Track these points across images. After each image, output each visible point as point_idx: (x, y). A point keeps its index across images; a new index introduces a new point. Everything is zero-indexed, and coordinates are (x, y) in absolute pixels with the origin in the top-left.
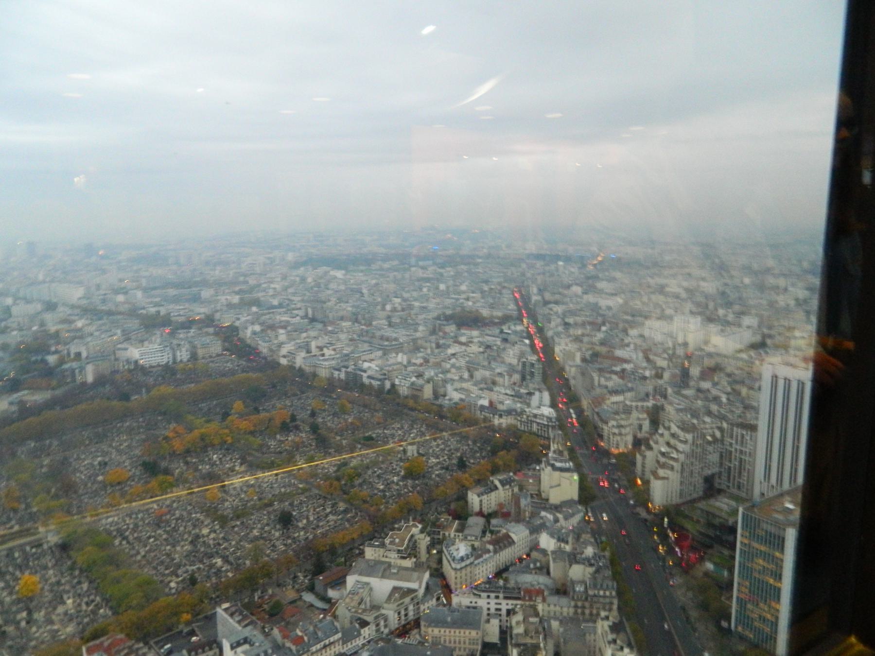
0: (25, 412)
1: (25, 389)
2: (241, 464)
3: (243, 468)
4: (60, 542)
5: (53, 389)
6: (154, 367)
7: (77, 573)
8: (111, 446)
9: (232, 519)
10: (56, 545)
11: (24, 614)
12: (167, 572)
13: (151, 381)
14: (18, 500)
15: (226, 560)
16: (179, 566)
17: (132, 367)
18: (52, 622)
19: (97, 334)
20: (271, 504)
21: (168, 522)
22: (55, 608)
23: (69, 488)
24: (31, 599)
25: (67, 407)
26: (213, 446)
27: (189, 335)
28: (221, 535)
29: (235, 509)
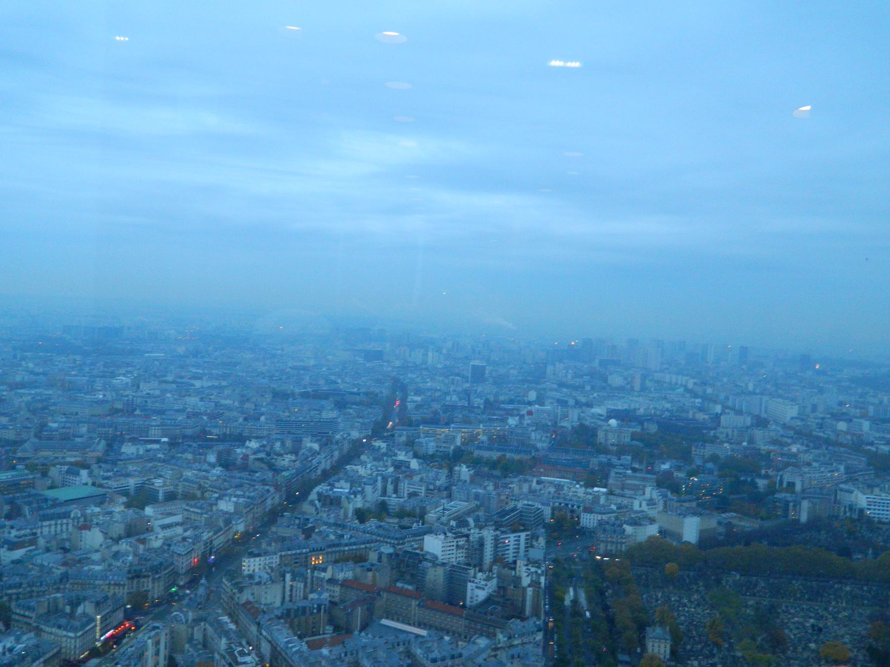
0: (731, 537)
1: (735, 511)
5: (762, 519)
6: (884, 523)
8: (826, 609)
17: (855, 516)
19: (815, 464)
25: (776, 544)
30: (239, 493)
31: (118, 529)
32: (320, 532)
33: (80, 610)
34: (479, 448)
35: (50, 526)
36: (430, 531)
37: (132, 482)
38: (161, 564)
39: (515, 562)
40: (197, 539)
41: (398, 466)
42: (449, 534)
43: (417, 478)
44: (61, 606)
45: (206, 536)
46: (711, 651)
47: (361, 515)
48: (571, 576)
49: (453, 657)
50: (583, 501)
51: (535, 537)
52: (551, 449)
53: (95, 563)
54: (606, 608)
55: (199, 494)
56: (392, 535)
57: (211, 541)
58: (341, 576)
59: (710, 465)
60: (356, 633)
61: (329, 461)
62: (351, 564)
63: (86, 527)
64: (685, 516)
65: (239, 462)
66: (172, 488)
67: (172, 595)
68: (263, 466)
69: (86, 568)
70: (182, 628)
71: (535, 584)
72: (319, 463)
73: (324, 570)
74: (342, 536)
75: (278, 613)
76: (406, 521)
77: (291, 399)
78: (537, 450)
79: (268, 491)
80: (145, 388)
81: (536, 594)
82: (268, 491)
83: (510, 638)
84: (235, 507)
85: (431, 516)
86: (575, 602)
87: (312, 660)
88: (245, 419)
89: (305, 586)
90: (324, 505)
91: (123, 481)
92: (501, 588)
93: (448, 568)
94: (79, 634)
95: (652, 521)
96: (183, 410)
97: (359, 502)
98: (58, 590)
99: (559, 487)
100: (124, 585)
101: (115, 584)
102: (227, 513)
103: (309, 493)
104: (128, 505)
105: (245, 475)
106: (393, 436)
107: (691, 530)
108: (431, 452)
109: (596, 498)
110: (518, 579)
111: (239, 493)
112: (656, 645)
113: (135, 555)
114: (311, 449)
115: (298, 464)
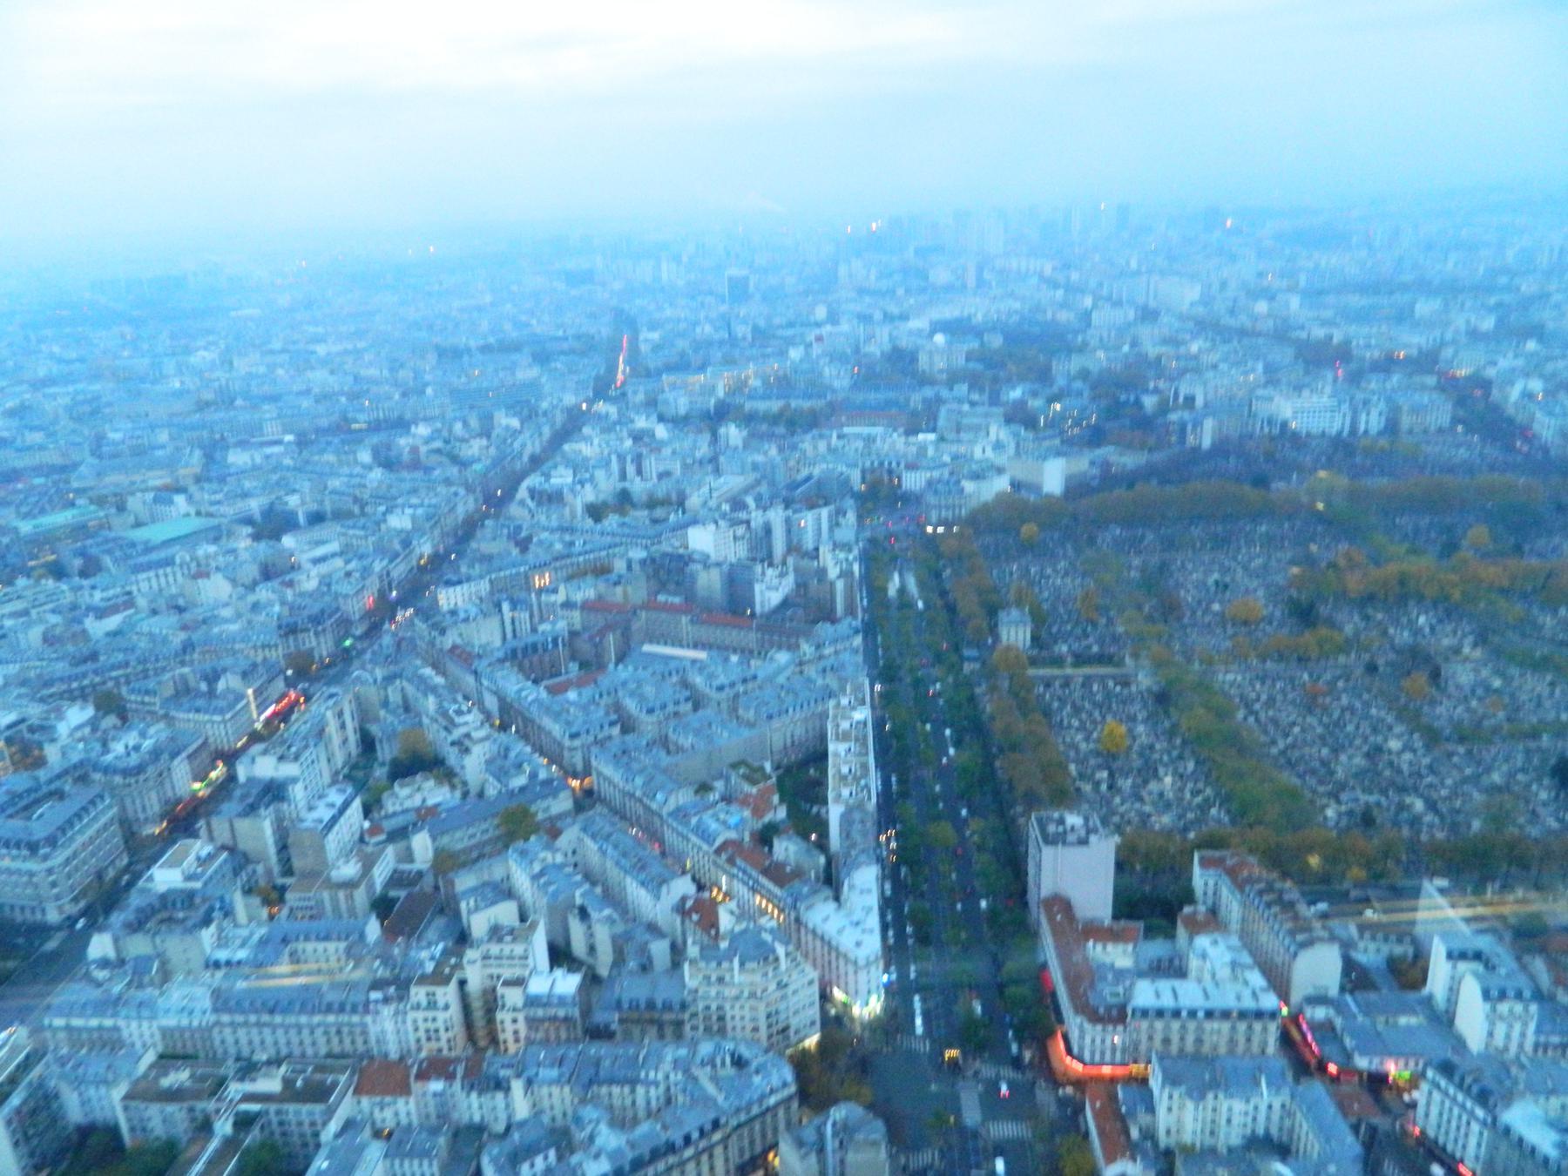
0: (1109, 478)
2: (1475, 645)
3: (1478, 653)
4: (1155, 688)
7: (1178, 741)
8: (1235, 558)
9: (1448, 740)
10: (1149, 690)
11: (1105, 774)
12: (1321, 789)
13: (1308, 460)
14: (1097, 608)
15: (1432, 806)
16: (1342, 787)
18: (1141, 800)
20: (1535, 735)
21: (1325, 709)
22: (1146, 782)
23: (1169, 609)
24: (1114, 757)
25: (1169, 482)
26: (1420, 598)
27: (1388, 386)
28: (1426, 761)
29: (1457, 725)
30: (414, 501)
31: (252, 571)
32: (541, 542)
33: (221, 685)
34: (751, 398)
35: (149, 579)
36: (695, 522)
37: (255, 505)
38: (322, 612)
39: (817, 549)
40: (366, 572)
41: (637, 437)
42: (721, 523)
43: (667, 451)
44: (192, 684)
45: (378, 566)
46: (1084, 631)
47: (596, 512)
48: (894, 559)
49: (745, 681)
50: (905, 455)
51: (841, 512)
52: (855, 386)
53: (226, 621)
54: (944, 594)
55: (356, 510)
56: (642, 533)
57: (388, 574)
58: (578, 597)
59: (1078, 385)
60: (611, 666)
61: (537, 443)
62: (590, 579)
63: (202, 574)
64: (1045, 459)
65: (406, 457)
66: (314, 507)
67: (347, 650)
68: (444, 459)
69: (216, 630)
70: (372, 694)
71: (846, 574)
72: (523, 446)
73: (555, 591)
74: (572, 544)
75: (500, 654)
76: (659, 512)
77: (466, 358)
78: (834, 391)
79: (456, 494)
80: (241, 365)
81: (849, 590)
82: (456, 494)
83: (818, 647)
84: (413, 523)
85: (694, 501)
86: (902, 590)
87: (556, 708)
88: (404, 395)
89: (531, 616)
90: (540, 504)
91: (240, 505)
92: (801, 586)
93: (725, 568)
94: (228, 716)
95: (1000, 471)
96: (308, 392)
97: (589, 495)
98: (183, 663)
99: (870, 440)
100: (276, 646)
101: (263, 647)
102: (402, 531)
103: (516, 490)
104: (257, 537)
105: (418, 475)
106: (624, 394)
107: (1053, 477)
108: (682, 411)
109: (922, 449)
110: (822, 572)
111: (414, 501)
112: (1013, 633)
113: (283, 603)
114: (507, 428)
115: (492, 451)
